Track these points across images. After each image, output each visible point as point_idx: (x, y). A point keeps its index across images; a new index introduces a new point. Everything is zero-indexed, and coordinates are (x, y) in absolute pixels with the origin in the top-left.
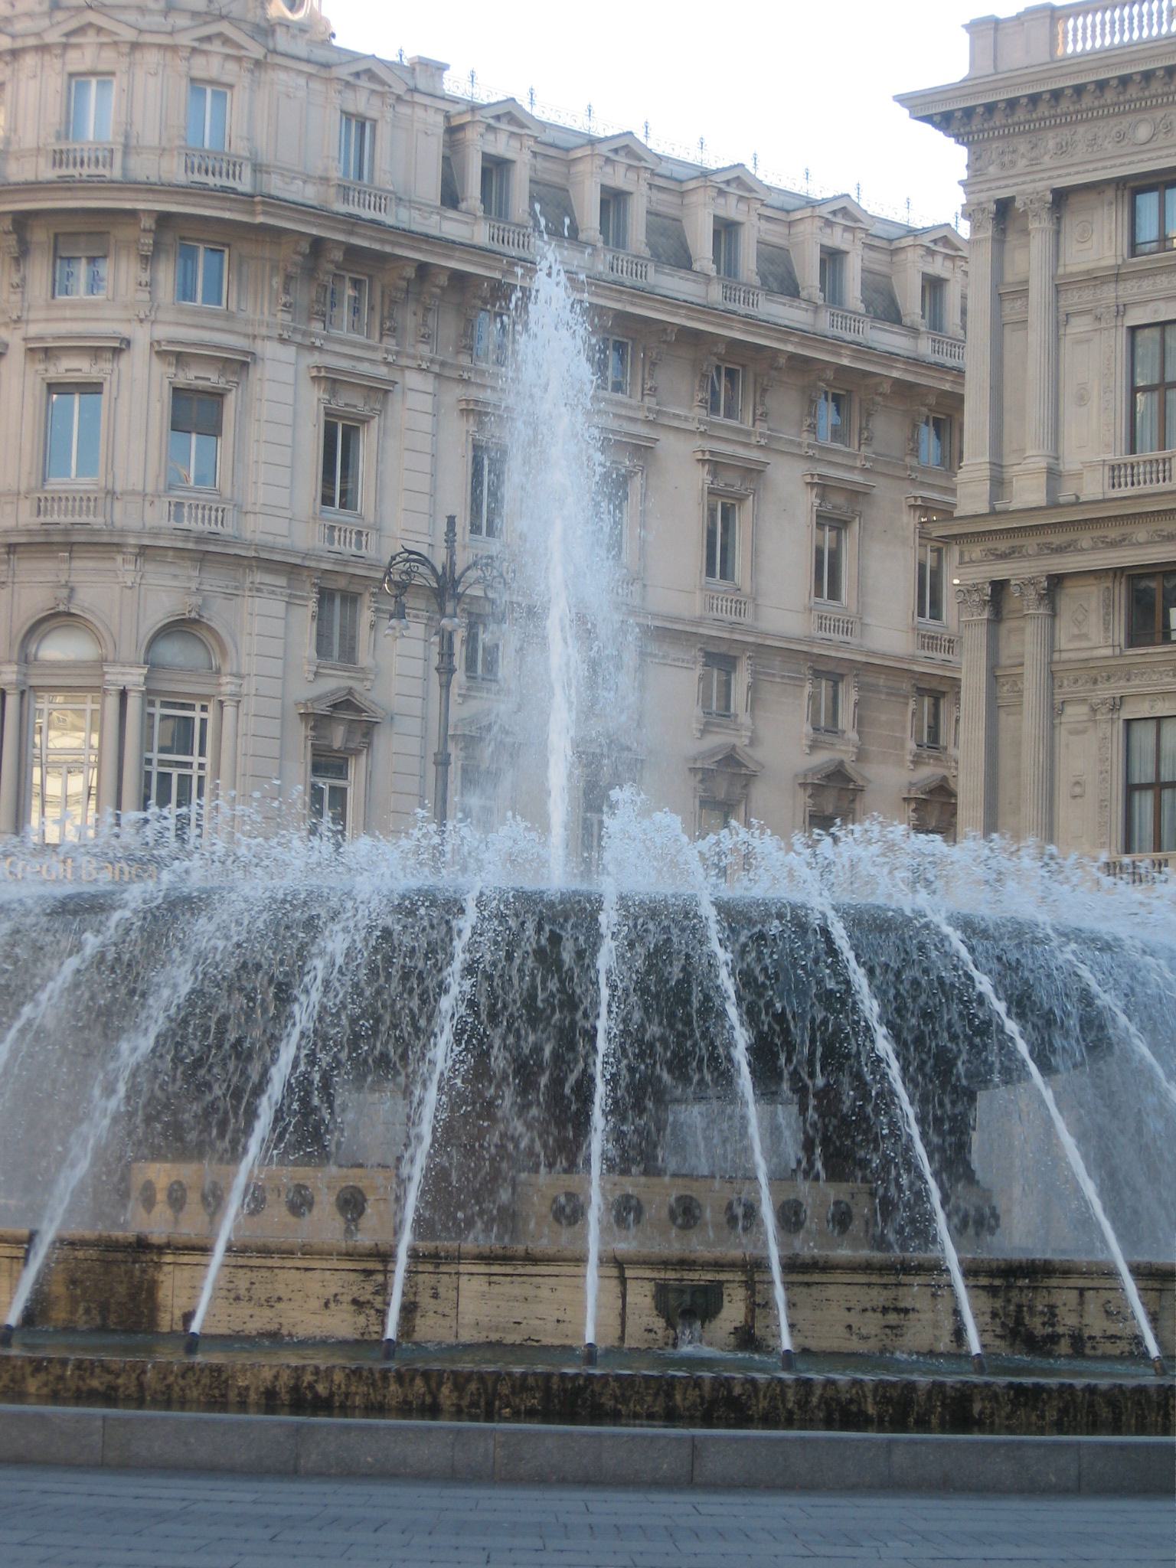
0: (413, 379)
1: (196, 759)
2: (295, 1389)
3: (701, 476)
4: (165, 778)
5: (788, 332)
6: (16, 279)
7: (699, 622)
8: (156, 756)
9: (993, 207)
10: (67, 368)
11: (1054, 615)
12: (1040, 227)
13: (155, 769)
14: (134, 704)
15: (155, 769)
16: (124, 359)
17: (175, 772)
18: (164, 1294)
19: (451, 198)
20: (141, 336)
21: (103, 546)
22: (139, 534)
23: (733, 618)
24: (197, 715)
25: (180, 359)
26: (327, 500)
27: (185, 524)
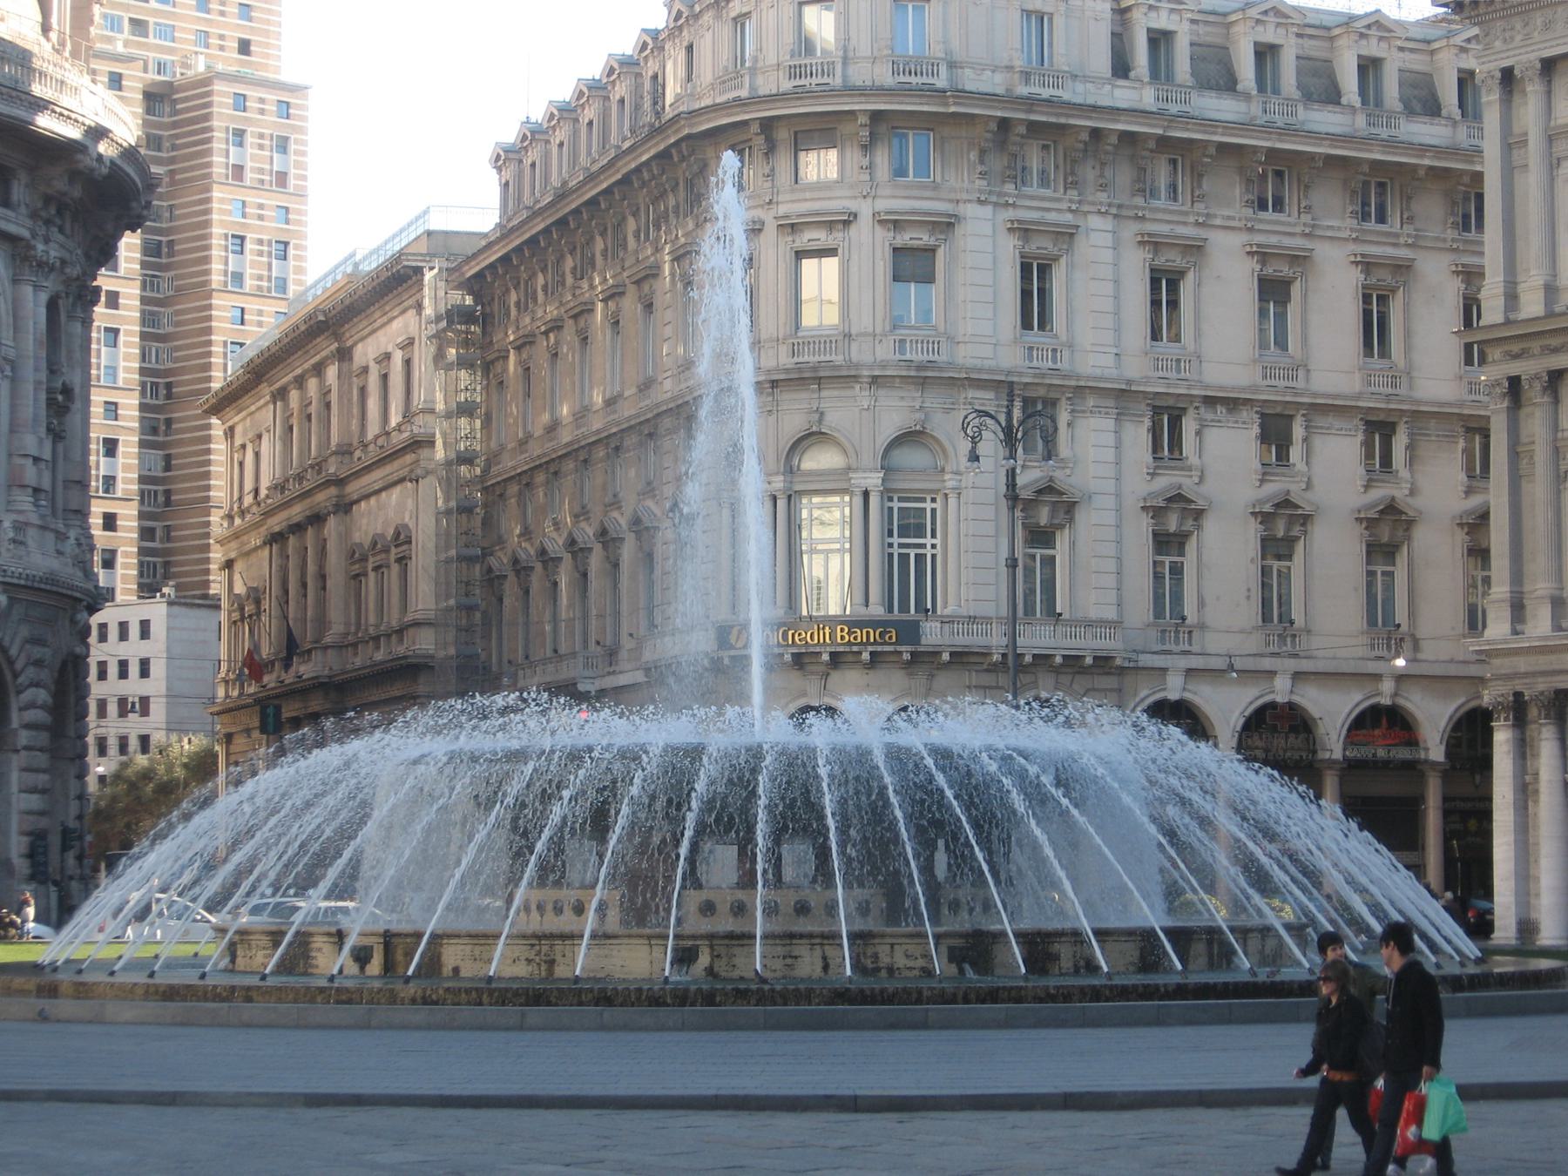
0: (1095, 222)
1: (928, 541)
2: (423, 997)
3: (1355, 276)
4: (904, 558)
5: (1423, 149)
6: (767, 171)
7: (1359, 396)
8: (896, 540)
9: (1498, 75)
10: (806, 238)
11: (1556, 401)
12: (1533, 89)
13: (896, 551)
14: (874, 500)
15: (896, 551)
16: (853, 229)
17: (912, 553)
18: (444, 958)
19: (1121, 68)
20: (865, 209)
21: (845, 378)
22: (871, 367)
23: (1390, 391)
24: (928, 506)
25: (897, 225)
26: (1026, 324)
27: (908, 356)
